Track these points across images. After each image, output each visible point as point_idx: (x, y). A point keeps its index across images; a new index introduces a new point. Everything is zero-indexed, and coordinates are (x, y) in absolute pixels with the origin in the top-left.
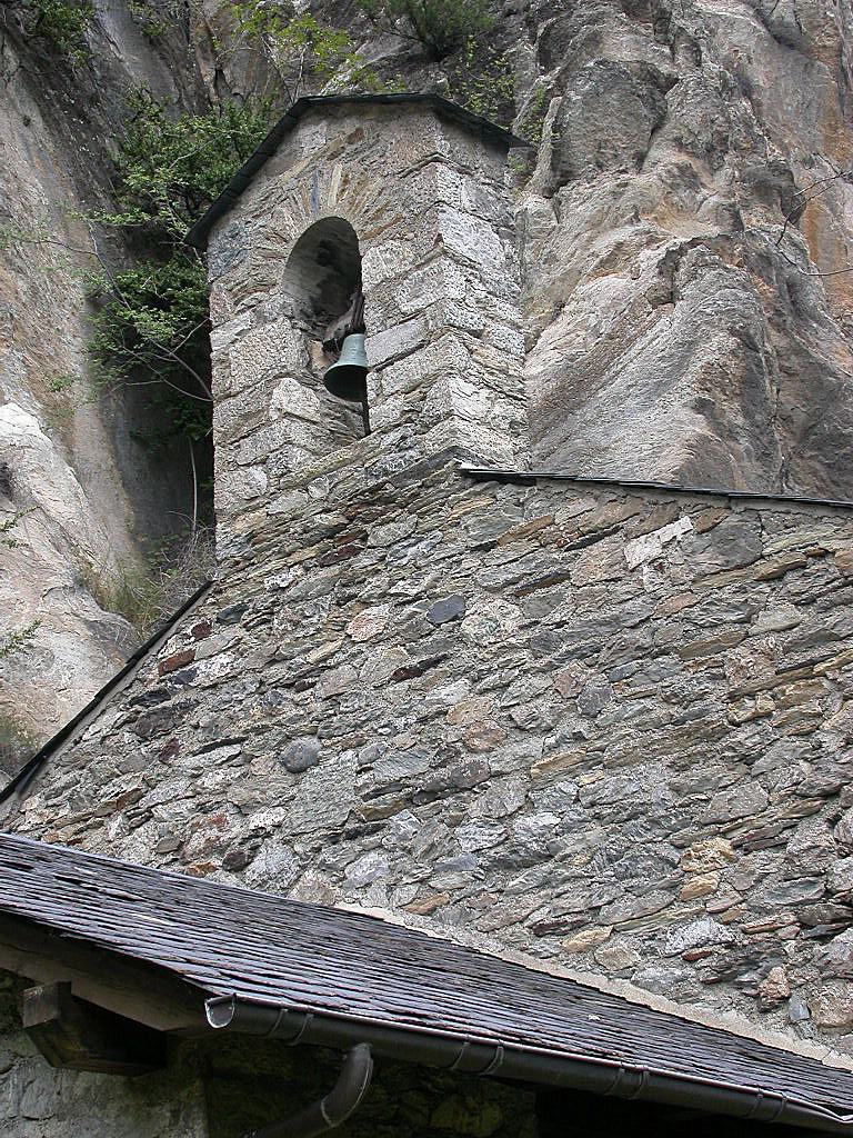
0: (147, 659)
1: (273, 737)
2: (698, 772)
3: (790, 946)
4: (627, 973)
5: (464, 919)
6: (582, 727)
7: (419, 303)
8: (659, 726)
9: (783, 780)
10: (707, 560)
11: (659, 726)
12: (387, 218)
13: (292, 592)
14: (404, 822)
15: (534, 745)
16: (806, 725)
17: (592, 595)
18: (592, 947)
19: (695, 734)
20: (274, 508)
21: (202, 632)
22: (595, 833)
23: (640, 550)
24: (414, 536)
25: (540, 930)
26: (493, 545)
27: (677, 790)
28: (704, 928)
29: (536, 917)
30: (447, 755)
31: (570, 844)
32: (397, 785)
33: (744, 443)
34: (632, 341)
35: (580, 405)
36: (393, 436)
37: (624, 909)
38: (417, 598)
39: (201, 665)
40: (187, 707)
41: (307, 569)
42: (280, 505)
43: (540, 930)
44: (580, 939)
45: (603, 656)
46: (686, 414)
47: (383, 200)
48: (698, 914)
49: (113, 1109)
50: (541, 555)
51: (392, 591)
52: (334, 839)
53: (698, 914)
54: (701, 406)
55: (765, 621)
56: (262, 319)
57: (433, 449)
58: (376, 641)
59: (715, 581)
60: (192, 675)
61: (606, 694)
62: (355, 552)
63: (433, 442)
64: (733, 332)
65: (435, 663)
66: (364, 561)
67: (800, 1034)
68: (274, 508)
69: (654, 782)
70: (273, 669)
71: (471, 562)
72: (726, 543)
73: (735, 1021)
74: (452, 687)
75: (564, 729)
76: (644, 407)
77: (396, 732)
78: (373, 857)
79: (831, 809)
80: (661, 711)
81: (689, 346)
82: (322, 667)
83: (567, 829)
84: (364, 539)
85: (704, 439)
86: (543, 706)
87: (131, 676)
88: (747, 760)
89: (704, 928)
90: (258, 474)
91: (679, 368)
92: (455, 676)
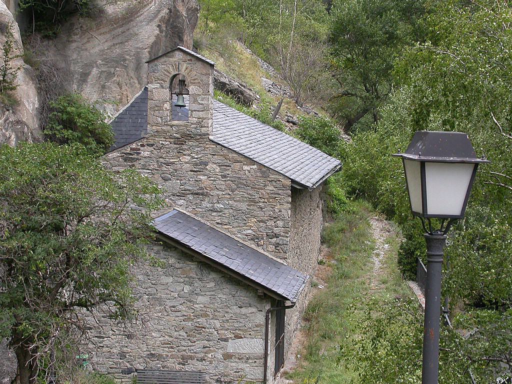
0: (128, 146)
1: (160, 172)
2: (252, 207)
3: (265, 238)
4: (234, 234)
5: (202, 217)
6: (231, 193)
7: (203, 102)
8: (246, 198)
9: (267, 213)
10: (258, 174)
11: (246, 198)
12: (196, 81)
13: (167, 146)
14: (191, 197)
15: (221, 193)
16: (273, 206)
17: (236, 172)
18: (228, 229)
19: (253, 202)
20: (163, 128)
21: (142, 146)
22: (231, 211)
23: (245, 168)
24: (197, 146)
25: (218, 223)
26: (215, 155)
27: (248, 209)
28: (250, 231)
29: (218, 221)
30: (201, 188)
31: (226, 211)
32: (189, 190)
33: (164, 34)
34: (145, 6)
35: (132, 20)
36: (195, 126)
37: (236, 224)
38: (197, 158)
39: (142, 152)
40: (138, 159)
41: (171, 143)
42: (165, 128)
43: (218, 223)
44: (225, 227)
45: (236, 182)
46: (155, 28)
47: (196, 77)
48: (249, 229)
49: (256, 299)
50: (225, 161)
51: (191, 155)
52: (174, 195)
53: (249, 229)
54: (159, 26)
55: (267, 188)
56: (162, 87)
57: (203, 132)
58: (186, 163)
59: (260, 178)
60: (140, 153)
61: (236, 190)
62: (183, 144)
63: (204, 130)
64: (168, 9)
65: (200, 171)
66: (184, 147)
67: (264, 251)
68: (163, 128)
69: (244, 206)
70: (161, 159)
71: (209, 156)
72: (262, 172)
73: (253, 246)
74: (204, 177)
75: (226, 192)
76: (147, 25)
77: (190, 181)
78: (183, 201)
79: (275, 220)
80: (247, 196)
81: (159, 11)
82: (173, 163)
83: (225, 209)
84: (185, 142)
85: (158, 34)
86: (223, 187)
87: (123, 148)
88: (262, 208)
89: (250, 231)
90: (159, 119)
91: (156, 16)
92: (204, 175)
